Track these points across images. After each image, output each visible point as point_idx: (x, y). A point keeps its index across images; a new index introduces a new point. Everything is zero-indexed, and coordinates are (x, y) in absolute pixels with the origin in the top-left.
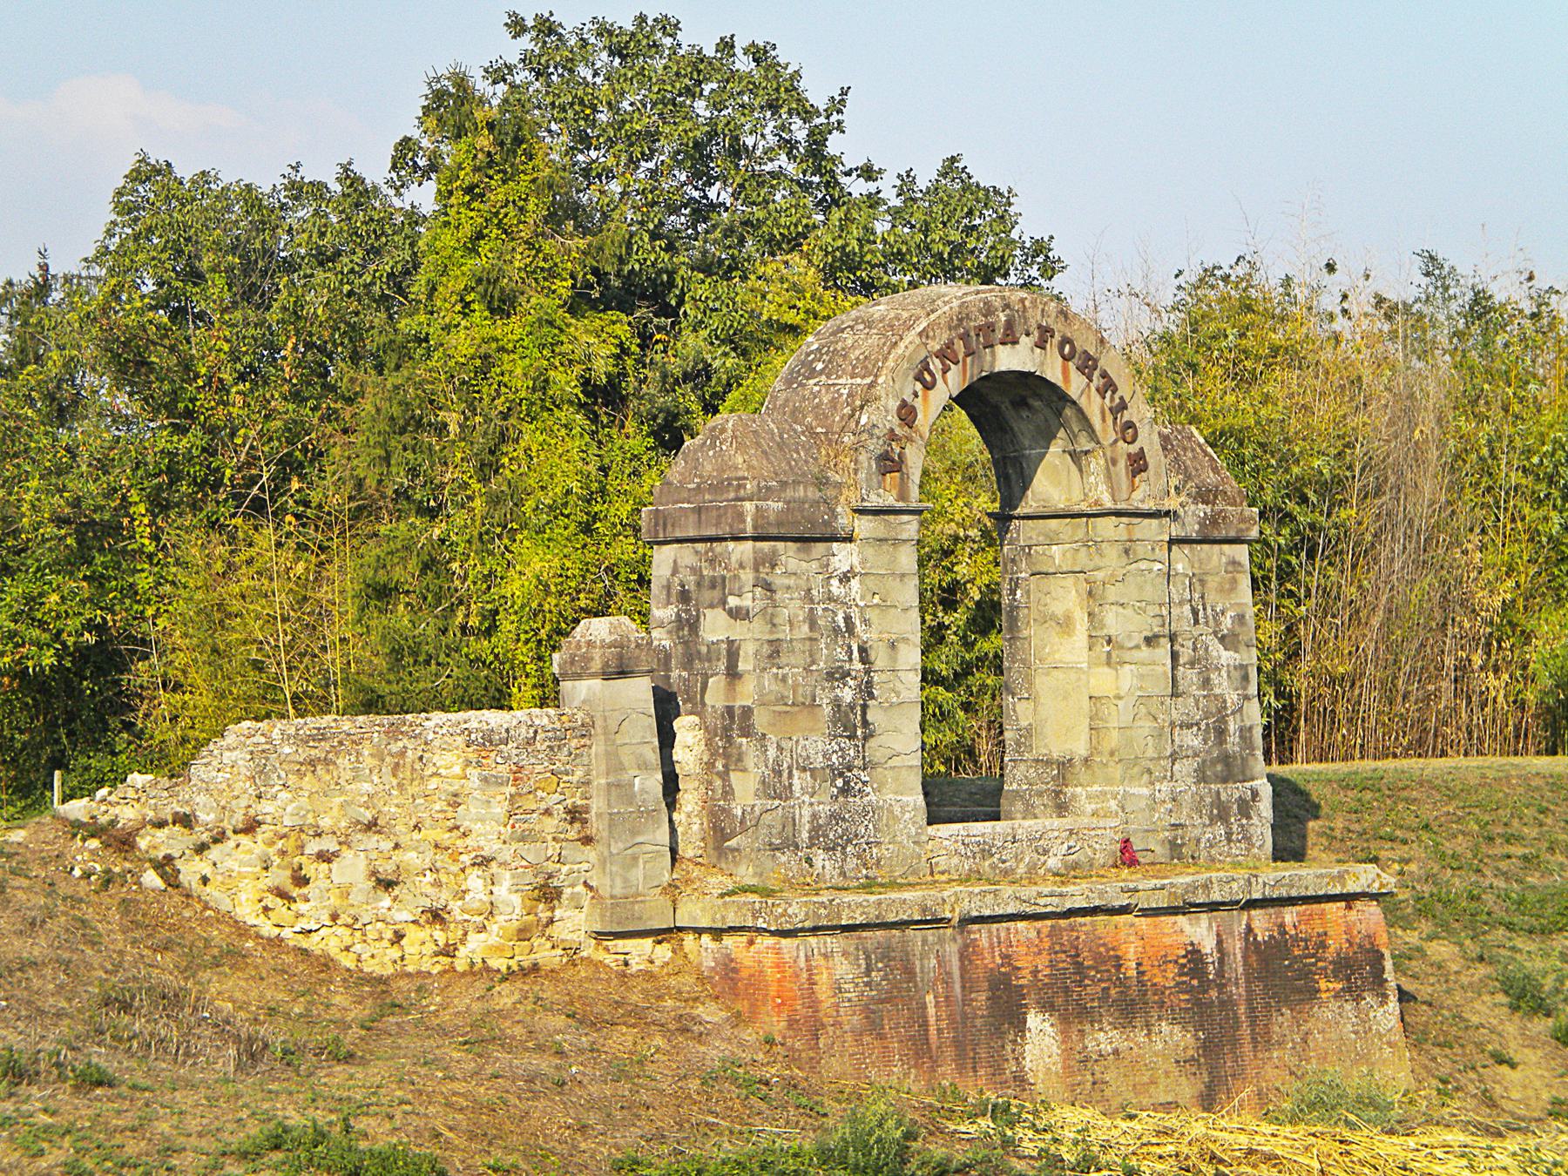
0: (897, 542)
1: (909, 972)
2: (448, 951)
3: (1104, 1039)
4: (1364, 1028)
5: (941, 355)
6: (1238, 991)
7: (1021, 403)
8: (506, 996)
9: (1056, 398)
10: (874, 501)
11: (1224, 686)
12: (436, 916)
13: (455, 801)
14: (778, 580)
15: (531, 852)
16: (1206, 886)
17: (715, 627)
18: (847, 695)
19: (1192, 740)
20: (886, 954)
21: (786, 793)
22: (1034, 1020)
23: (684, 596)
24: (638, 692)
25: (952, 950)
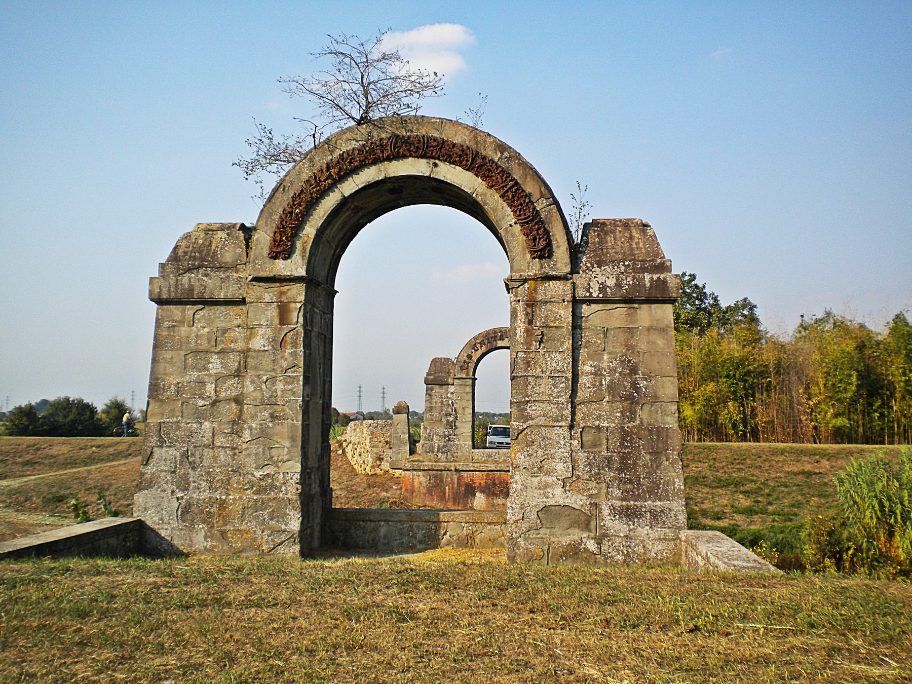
0: (466, 385)
1: (442, 481)
10: (459, 376)
14: (433, 393)
15: (375, 450)
18: (451, 419)
20: (435, 476)
22: (478, 494)
25: (455, 477)
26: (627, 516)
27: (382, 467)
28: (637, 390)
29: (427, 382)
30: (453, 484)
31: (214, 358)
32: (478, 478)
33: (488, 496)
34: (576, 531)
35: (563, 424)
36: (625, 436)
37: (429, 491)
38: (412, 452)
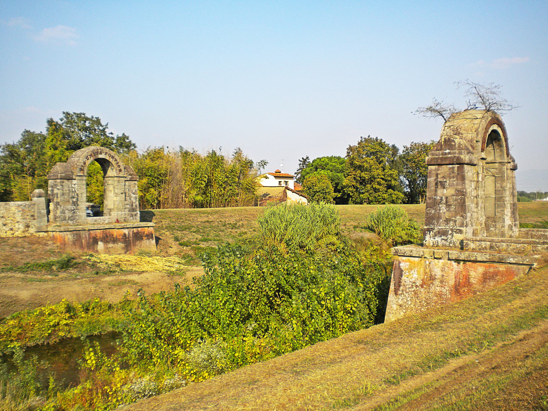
1: (80, 237)
2: (13, 234)
3: (110, 245)
6: (131, 239)
7: (105, 162)
8: (20, 240)
9: (109, 162)
10: (79, 174)
11: (133, 199)
12: (12, 229)
13: (14, 214)
15: (25, 221)
17: (56, 191)
18: (74, 200)
19: (128, 206)
20: (76, 234)
21: (65, 213)
22: (99, 243)
23: (52, 187)
24: (43, 199)
25: (87, 234)
30: (86, 238)
32: (99, 233)
37: (74, 243)
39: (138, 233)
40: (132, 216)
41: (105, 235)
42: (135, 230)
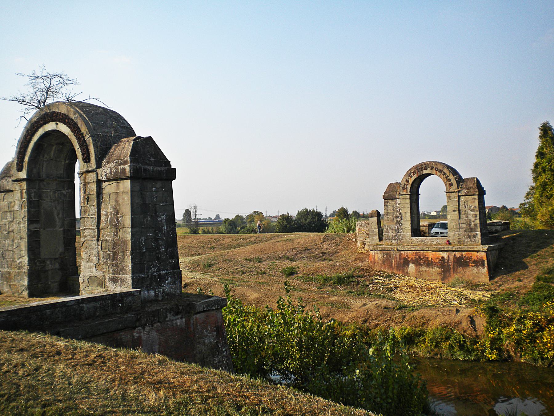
1: (390, 257)
3: (424, 269)
4: (478, 272)
5: (413, 173)
10: (402, 193)
11: (470, 217)
14: (388, 204)
16: (444, 248)
19: (464, 226)
20: (387, 254)
21: (389, 232)
22: (411, 265)
25: (398, 254)
26: (113, 281)
27: (365, 248)
28: (118, 222)
29: (384, 198)
30: (396, 258)
31: (9, 214)
33: (416, 265)
34: (99, 288)
35: (95, 239)
36: (115, 244)
38: (380, 239)
39: (461, 258)
40: (470, 237)
41: (417, 257)
42: (458, 254)
